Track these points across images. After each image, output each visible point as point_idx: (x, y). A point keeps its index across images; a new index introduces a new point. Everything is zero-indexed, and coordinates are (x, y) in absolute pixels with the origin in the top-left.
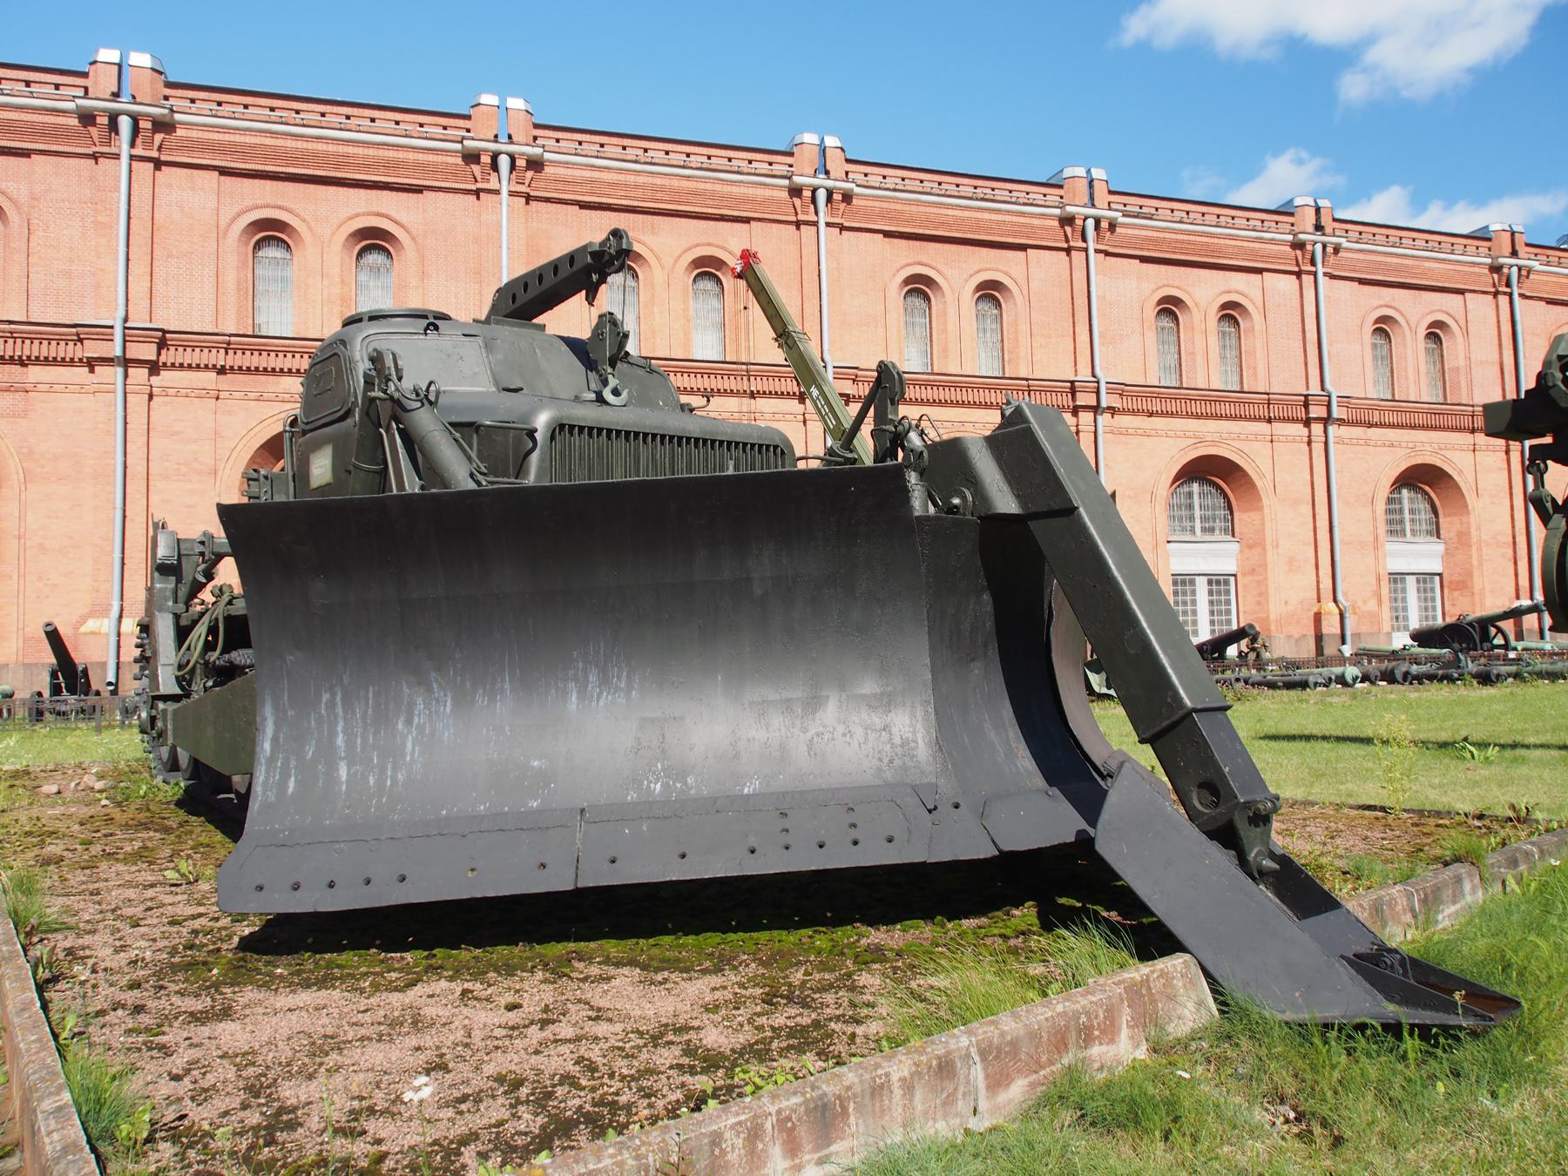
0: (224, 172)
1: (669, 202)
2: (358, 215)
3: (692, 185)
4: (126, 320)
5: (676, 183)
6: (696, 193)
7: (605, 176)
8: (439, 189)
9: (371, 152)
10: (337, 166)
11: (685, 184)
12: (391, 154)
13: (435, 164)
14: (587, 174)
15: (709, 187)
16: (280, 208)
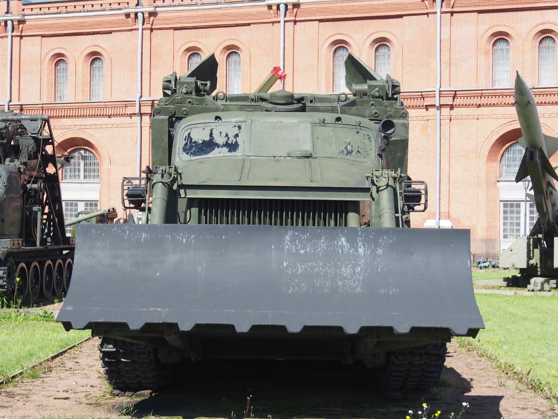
0: (43, 36)
1: (213, 21)
2: (88, 47)
3: (222, 12)
4: (10, 101)
5: (214, 12)
6: (224, 15)
7: (184, 14)
8: (118, 31)
9: (91, 19)
10: (81, 27)
11: (218, 12)
12: (98, 19)
13: (115, 20)
14: (176, 14)
15: (230, 11)
16: (61, 48)
